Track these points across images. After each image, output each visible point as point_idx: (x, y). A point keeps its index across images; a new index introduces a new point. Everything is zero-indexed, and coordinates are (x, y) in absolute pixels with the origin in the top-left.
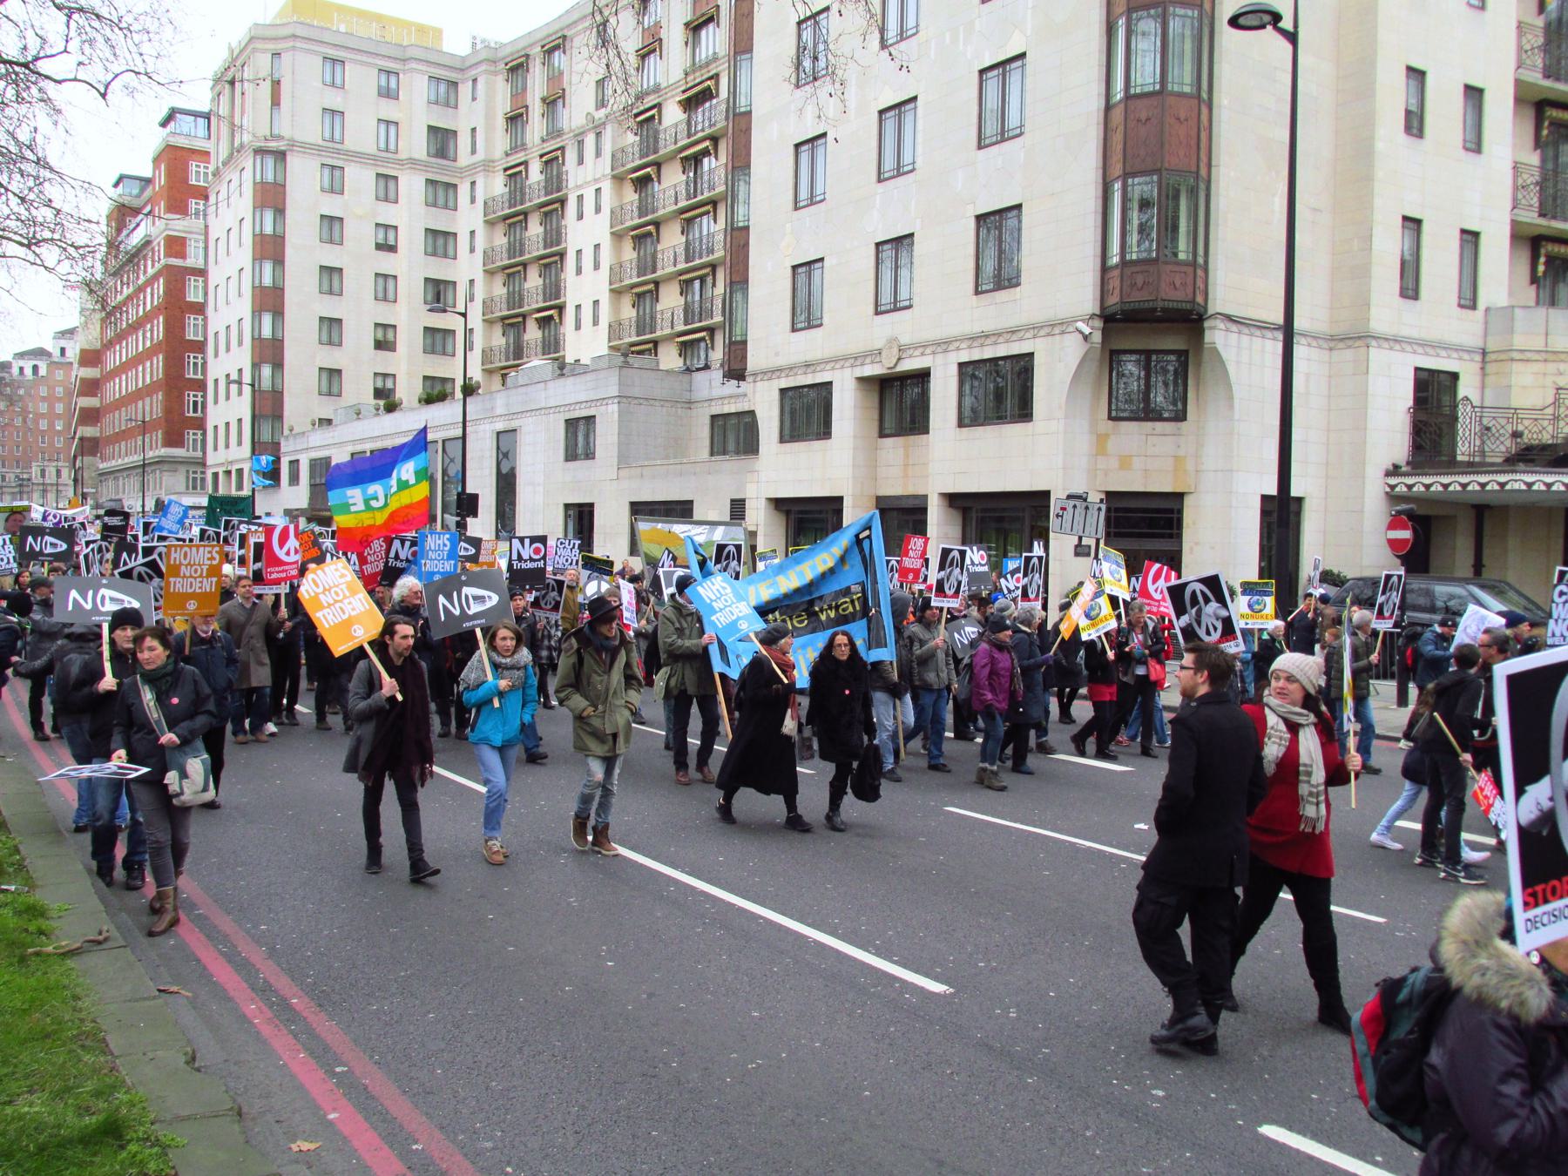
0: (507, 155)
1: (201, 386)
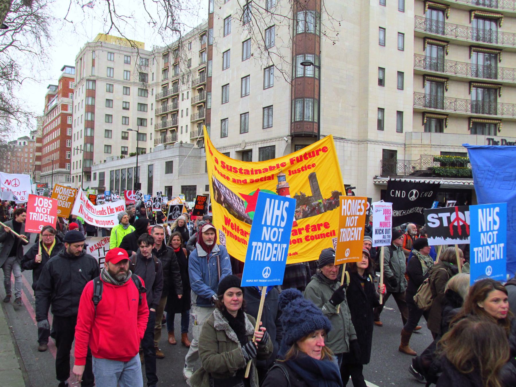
0: (163, 81)
1: (70, 149)
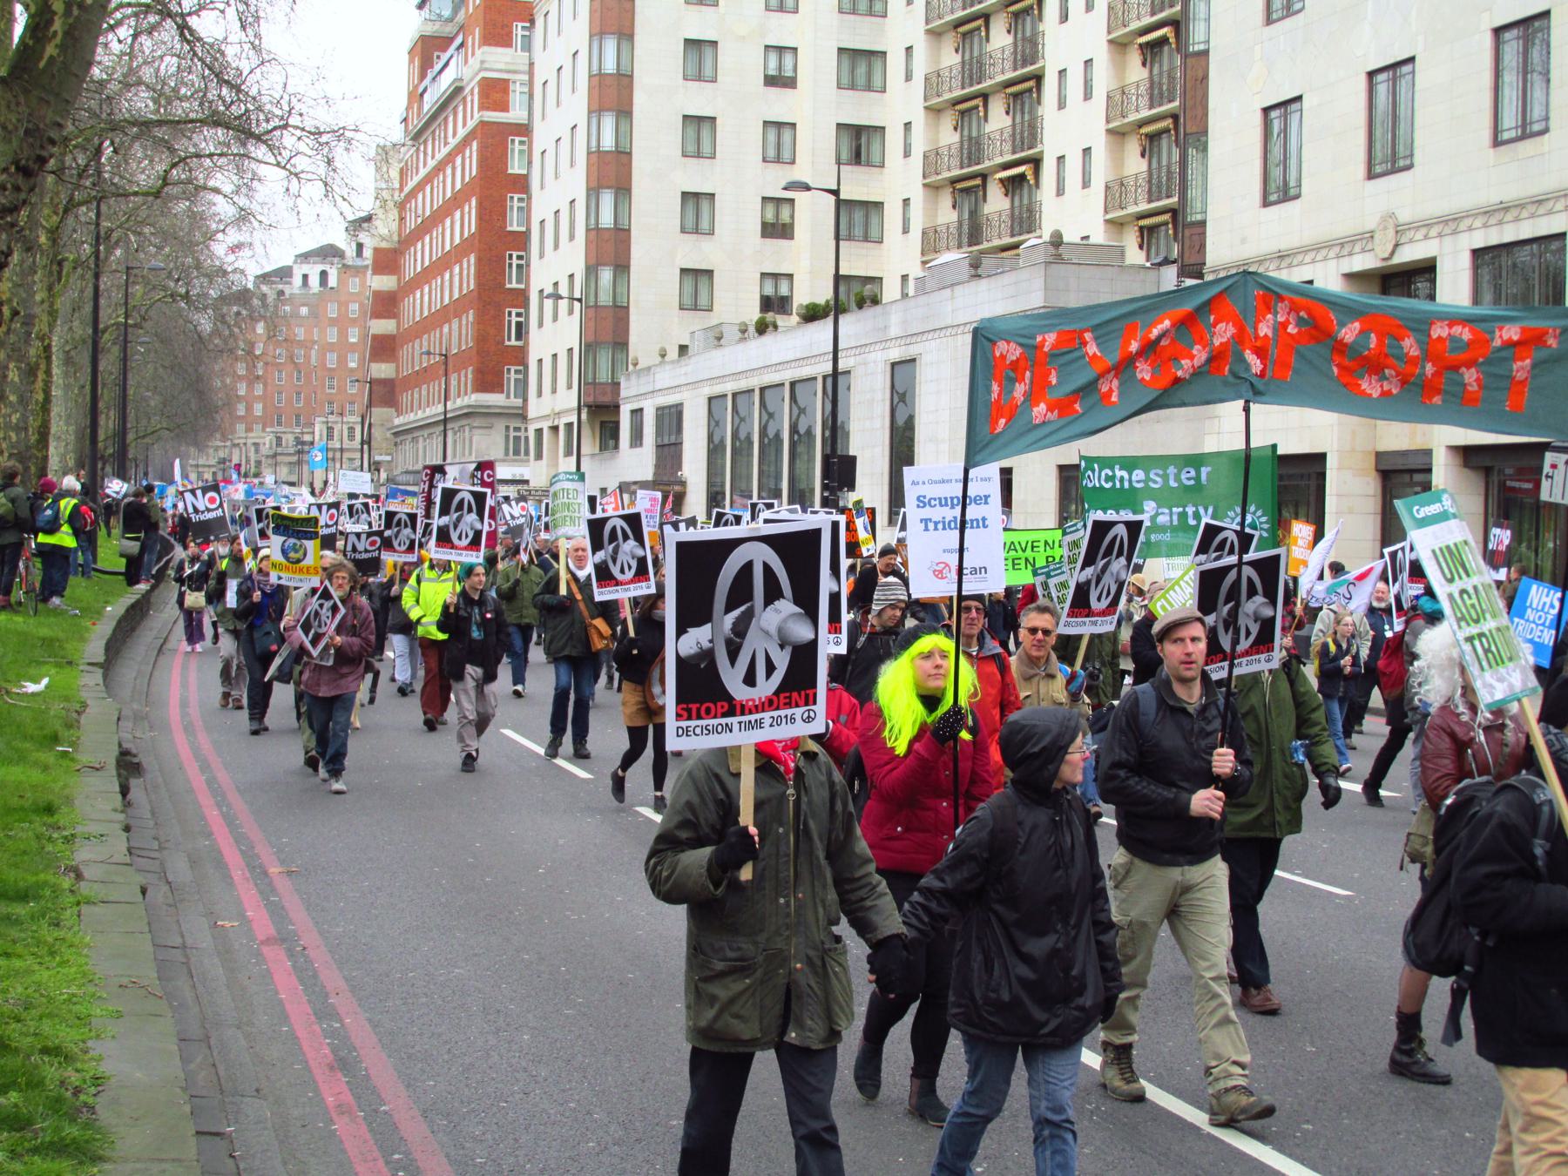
1: (521, 298)
